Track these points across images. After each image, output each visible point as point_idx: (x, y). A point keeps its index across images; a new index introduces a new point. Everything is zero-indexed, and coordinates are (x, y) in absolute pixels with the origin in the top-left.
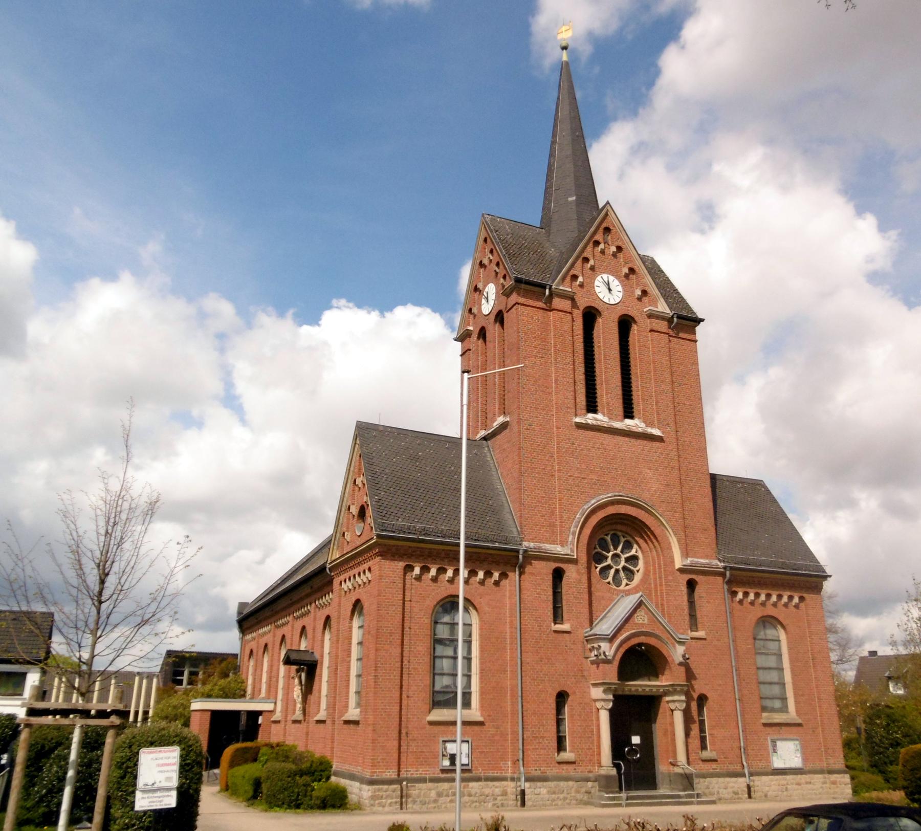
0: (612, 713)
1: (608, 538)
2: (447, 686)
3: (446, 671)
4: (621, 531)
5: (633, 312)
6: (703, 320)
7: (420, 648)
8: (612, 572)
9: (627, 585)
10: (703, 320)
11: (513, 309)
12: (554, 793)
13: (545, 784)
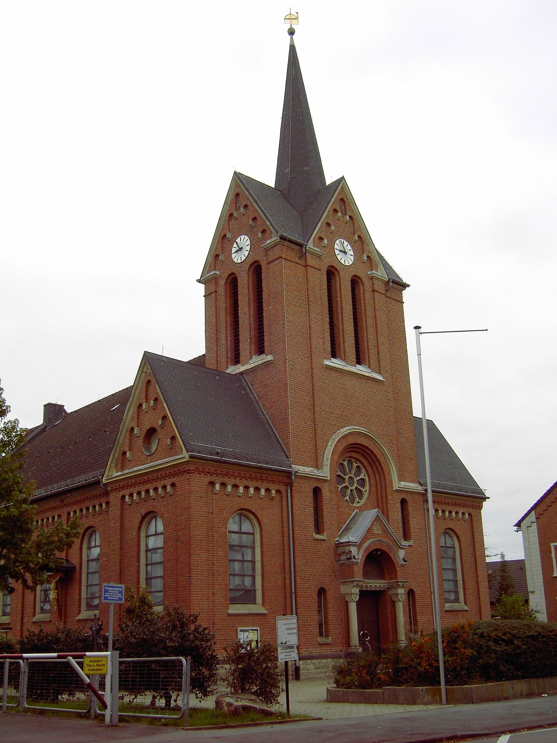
0: (359, 604)
1: (345, 463)
2: (238, 585)
3: (237, 572)
4: (354, 458)
5: (361, 274)
6: (408, 286)
7: (220, 553)
8: (349, 491)
9: (359, 502)
10: (408, 286)
11: (276, 262)
12: (319, 668)
13: (313, 661)
